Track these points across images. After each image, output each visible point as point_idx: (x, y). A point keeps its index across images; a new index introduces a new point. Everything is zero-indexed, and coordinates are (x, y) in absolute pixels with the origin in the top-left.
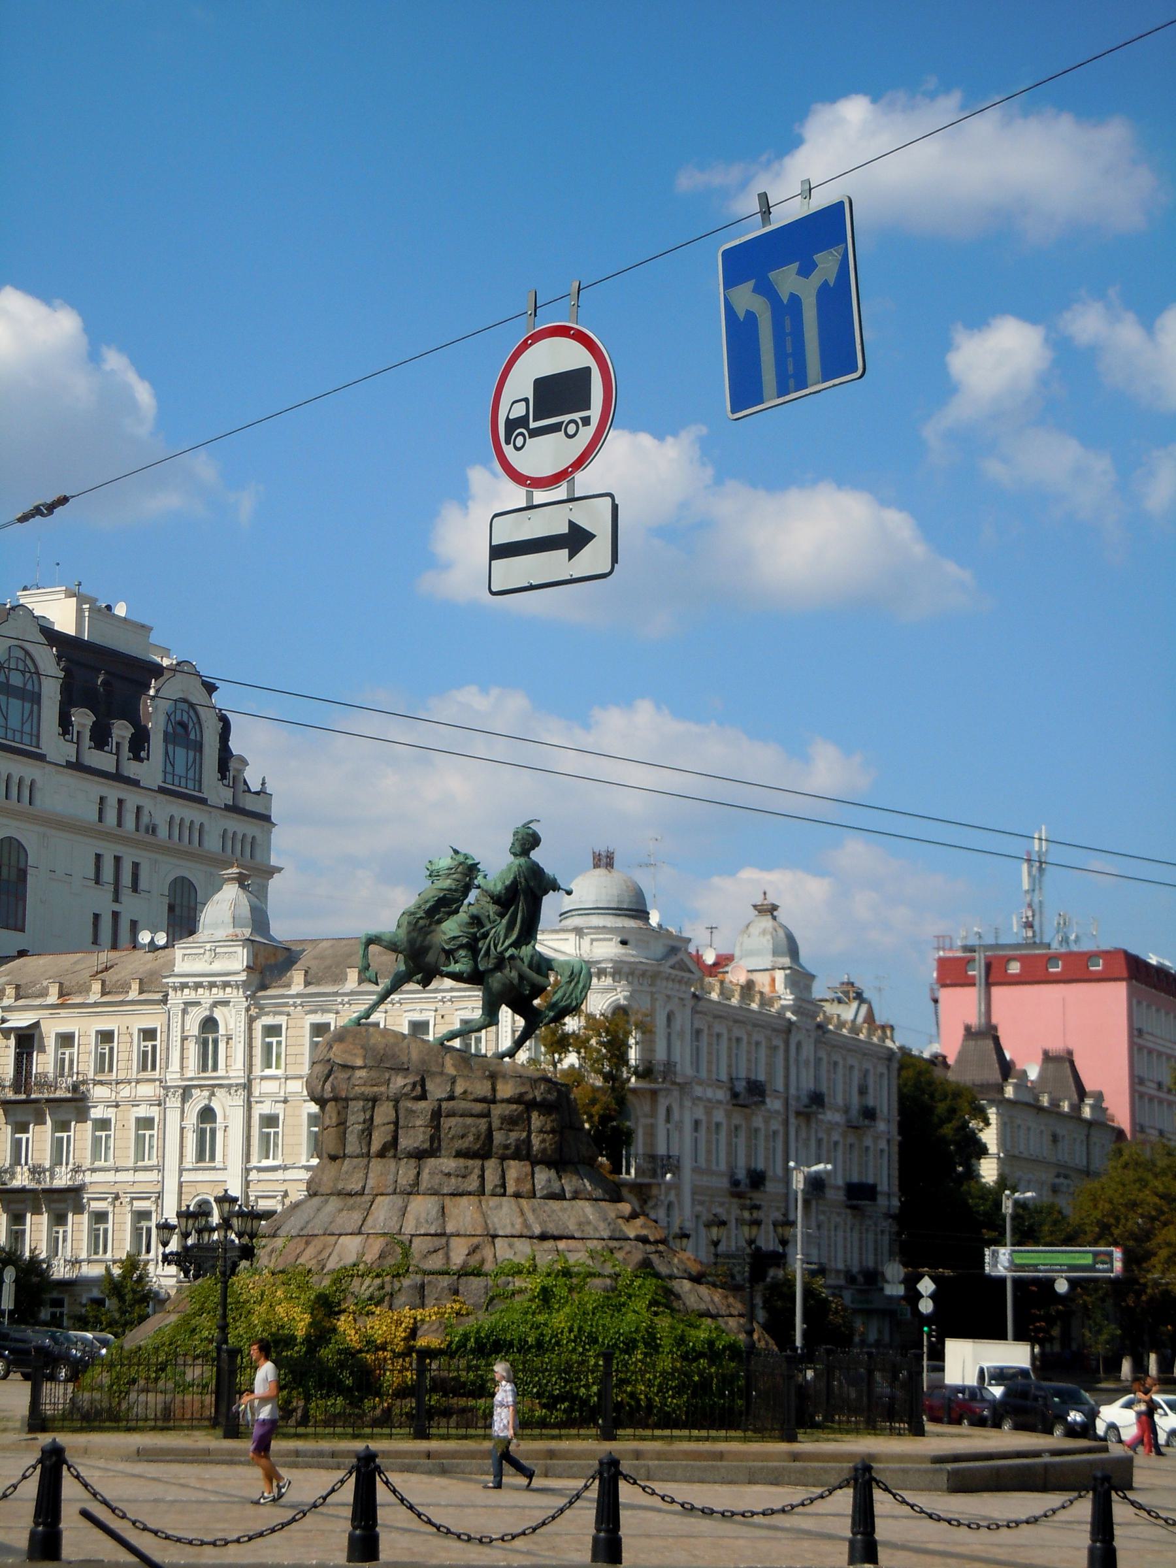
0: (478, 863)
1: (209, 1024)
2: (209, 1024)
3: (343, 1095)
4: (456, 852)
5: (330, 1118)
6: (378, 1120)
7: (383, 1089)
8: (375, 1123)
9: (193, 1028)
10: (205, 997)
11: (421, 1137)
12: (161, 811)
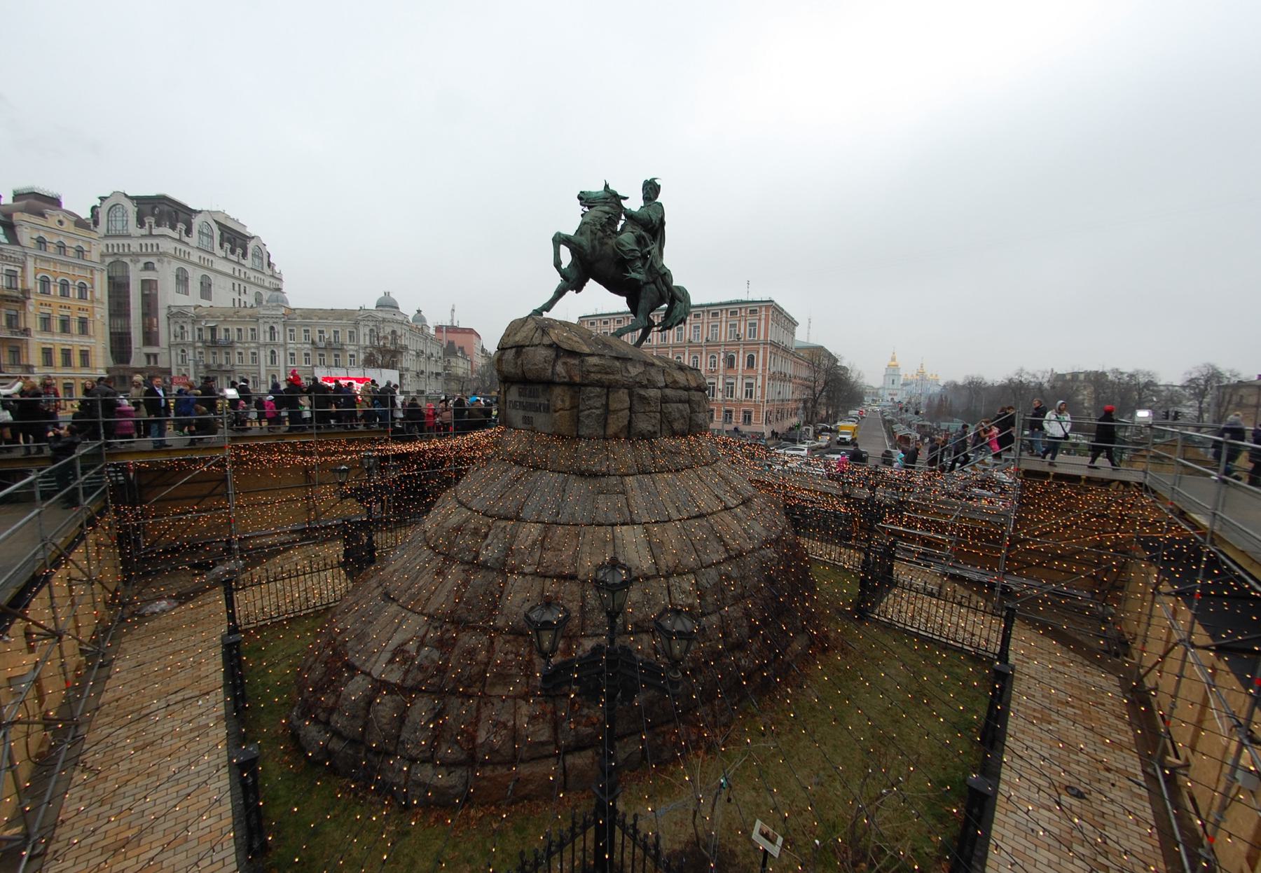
0: (625, 198)
1: (272, 328)
2: (272, 328)
3: (577, 379)
4: (607, 186)
5: (563, 401)
6: (613, 406)
7: (618, 377)
8: (611, 408)
9: (268, 329)
10: (271, 321)
12: (251, 274)
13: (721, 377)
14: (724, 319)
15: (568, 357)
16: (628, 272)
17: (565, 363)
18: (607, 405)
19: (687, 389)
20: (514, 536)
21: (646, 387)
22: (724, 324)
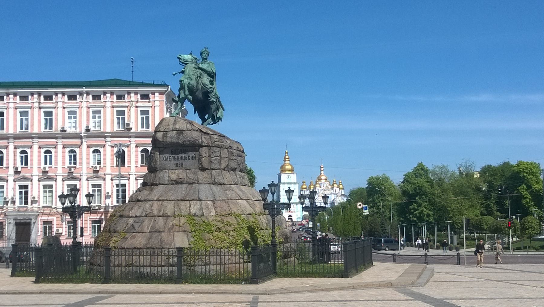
3: (211, 145)
5: (206, 153)
7: (224, 144)
11: (235, 163)
13: (108, 178)
14: (109, 104)
15: (205, 135)
16: (209, 97)
17: (205, 138)
18: (220, 155)
19: (240, 151)
20: (201, 205)
21: (231, 148)
22: (109, 110)
